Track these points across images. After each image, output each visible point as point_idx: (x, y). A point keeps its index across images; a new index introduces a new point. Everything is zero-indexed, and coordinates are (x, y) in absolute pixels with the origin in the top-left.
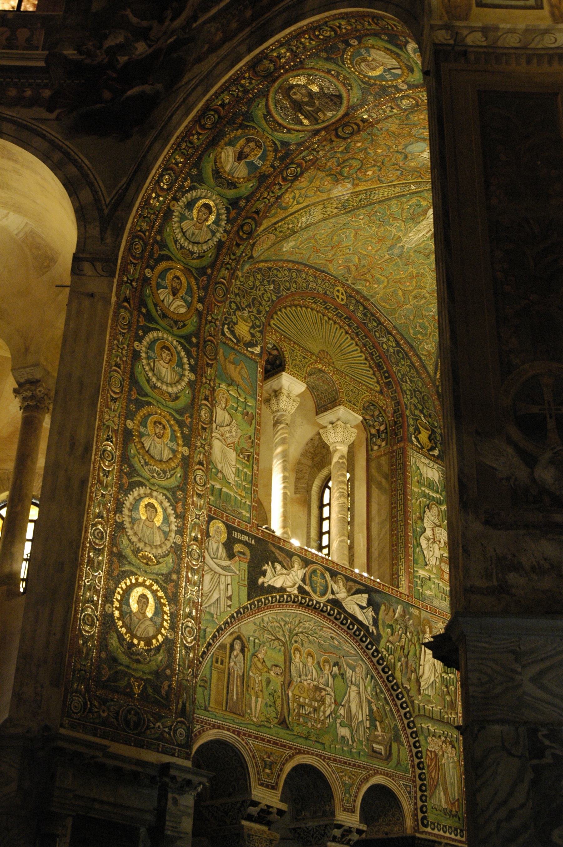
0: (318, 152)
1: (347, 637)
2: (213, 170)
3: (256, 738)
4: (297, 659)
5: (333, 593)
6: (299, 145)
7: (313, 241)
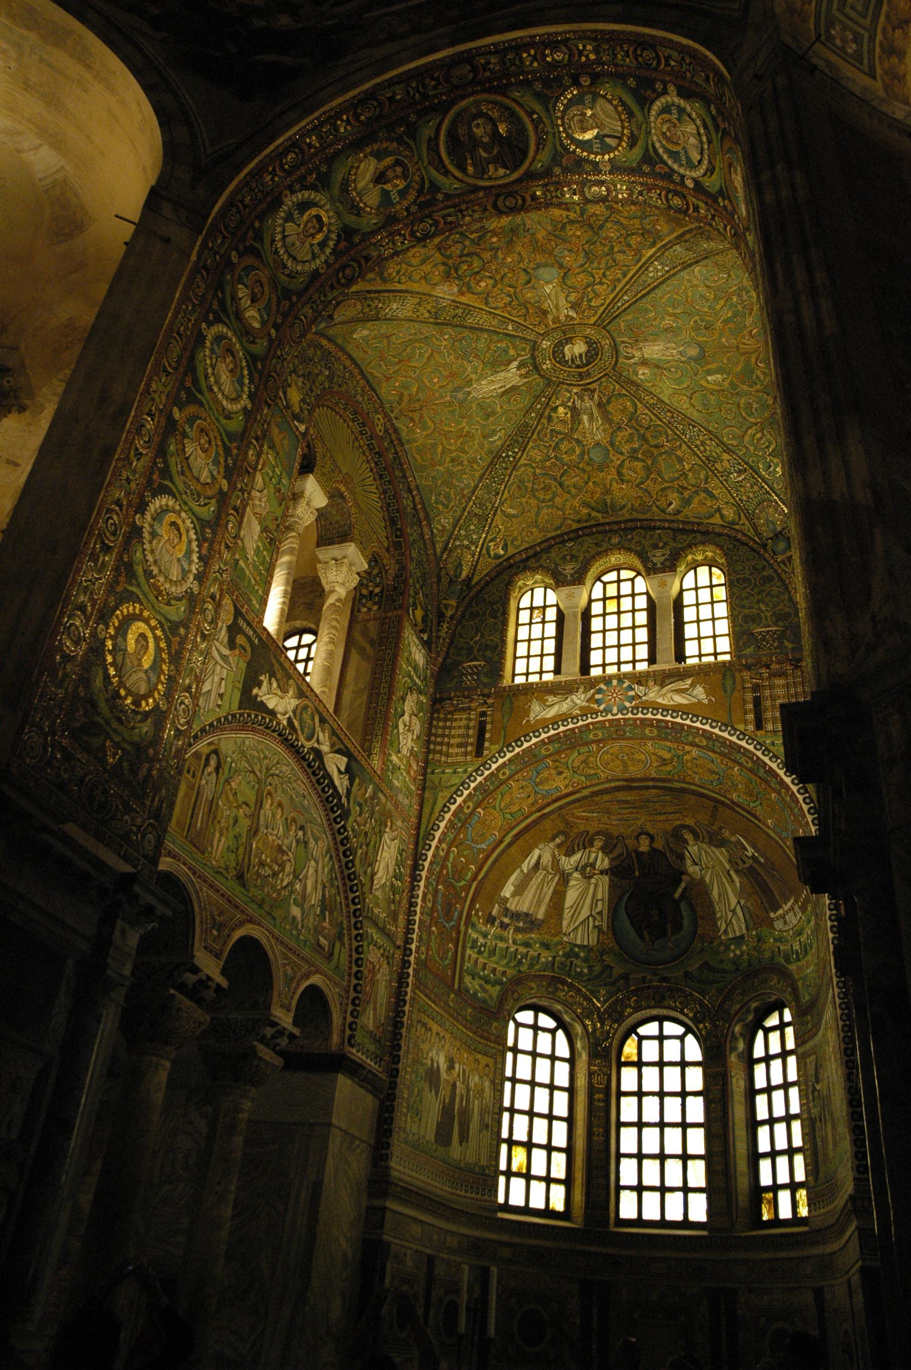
0: (464, 216)
1: (317, 801)
3: (211, 886)
4: (267, 805)
5: (318, 741)
6: (448, 197)
7: (385, 341)
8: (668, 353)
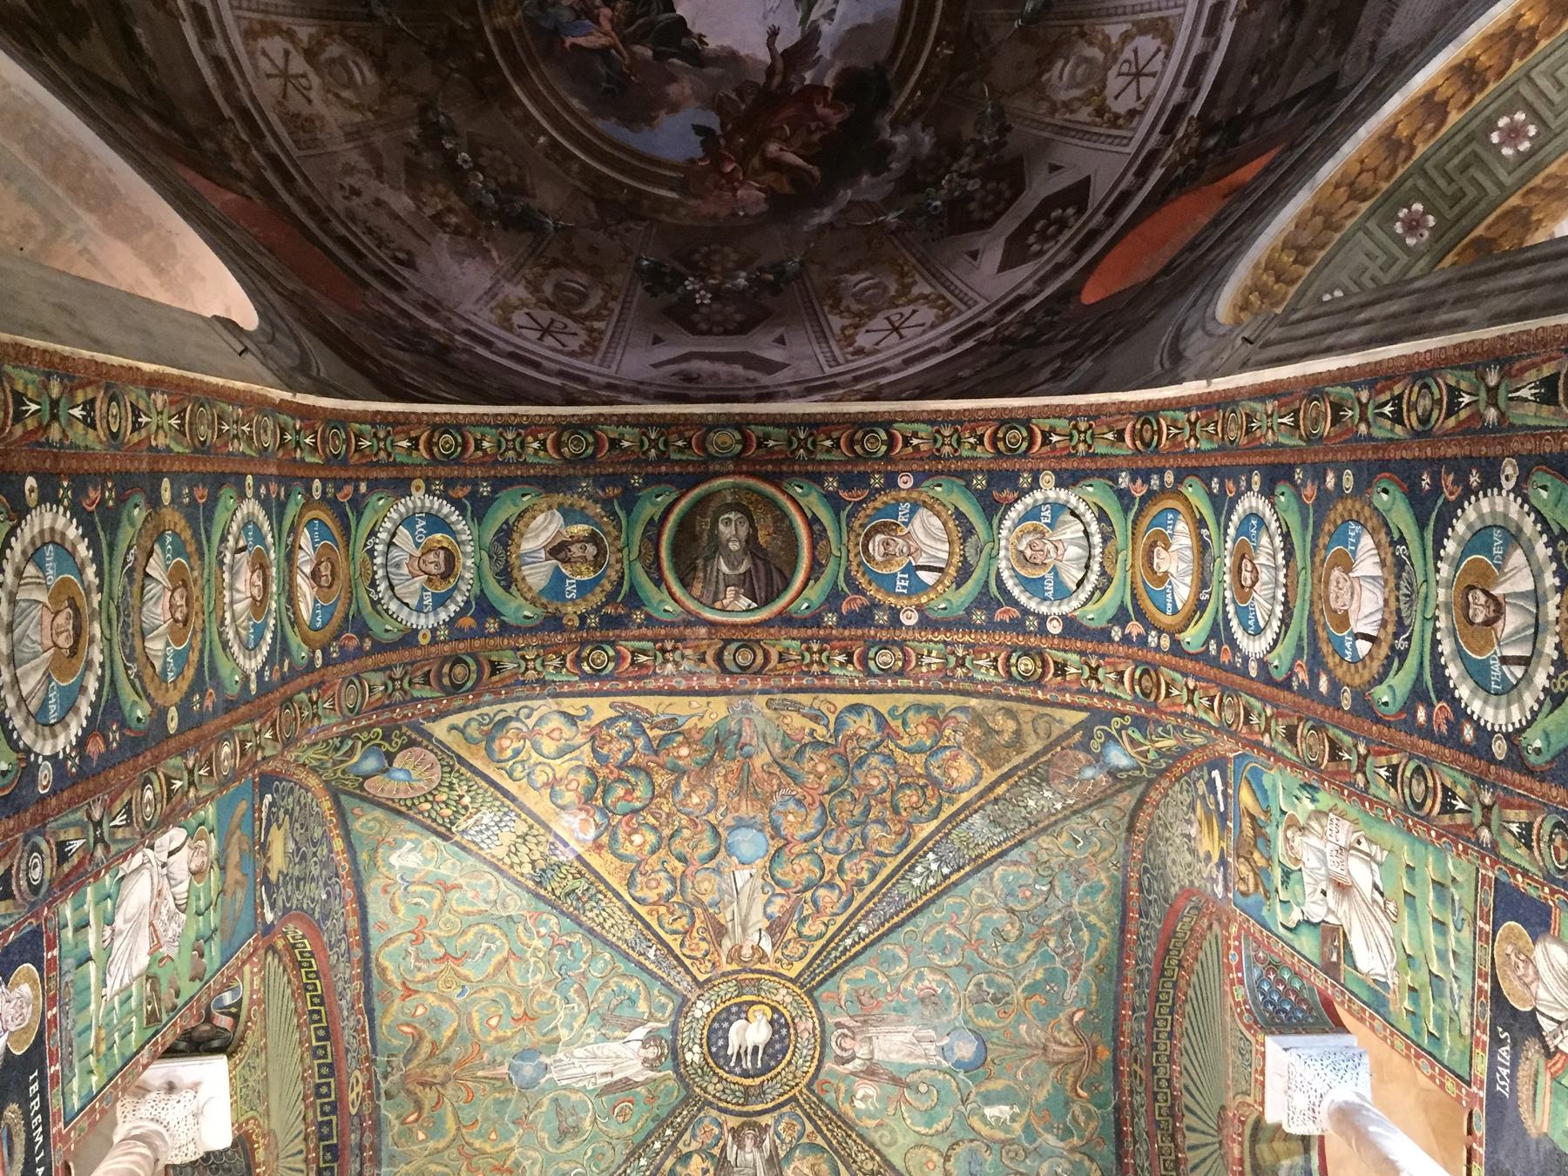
0: (666, 661)
2: (506, 522)
6: (650, 620)
8: (919, 1051)
